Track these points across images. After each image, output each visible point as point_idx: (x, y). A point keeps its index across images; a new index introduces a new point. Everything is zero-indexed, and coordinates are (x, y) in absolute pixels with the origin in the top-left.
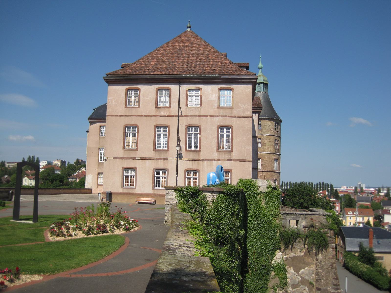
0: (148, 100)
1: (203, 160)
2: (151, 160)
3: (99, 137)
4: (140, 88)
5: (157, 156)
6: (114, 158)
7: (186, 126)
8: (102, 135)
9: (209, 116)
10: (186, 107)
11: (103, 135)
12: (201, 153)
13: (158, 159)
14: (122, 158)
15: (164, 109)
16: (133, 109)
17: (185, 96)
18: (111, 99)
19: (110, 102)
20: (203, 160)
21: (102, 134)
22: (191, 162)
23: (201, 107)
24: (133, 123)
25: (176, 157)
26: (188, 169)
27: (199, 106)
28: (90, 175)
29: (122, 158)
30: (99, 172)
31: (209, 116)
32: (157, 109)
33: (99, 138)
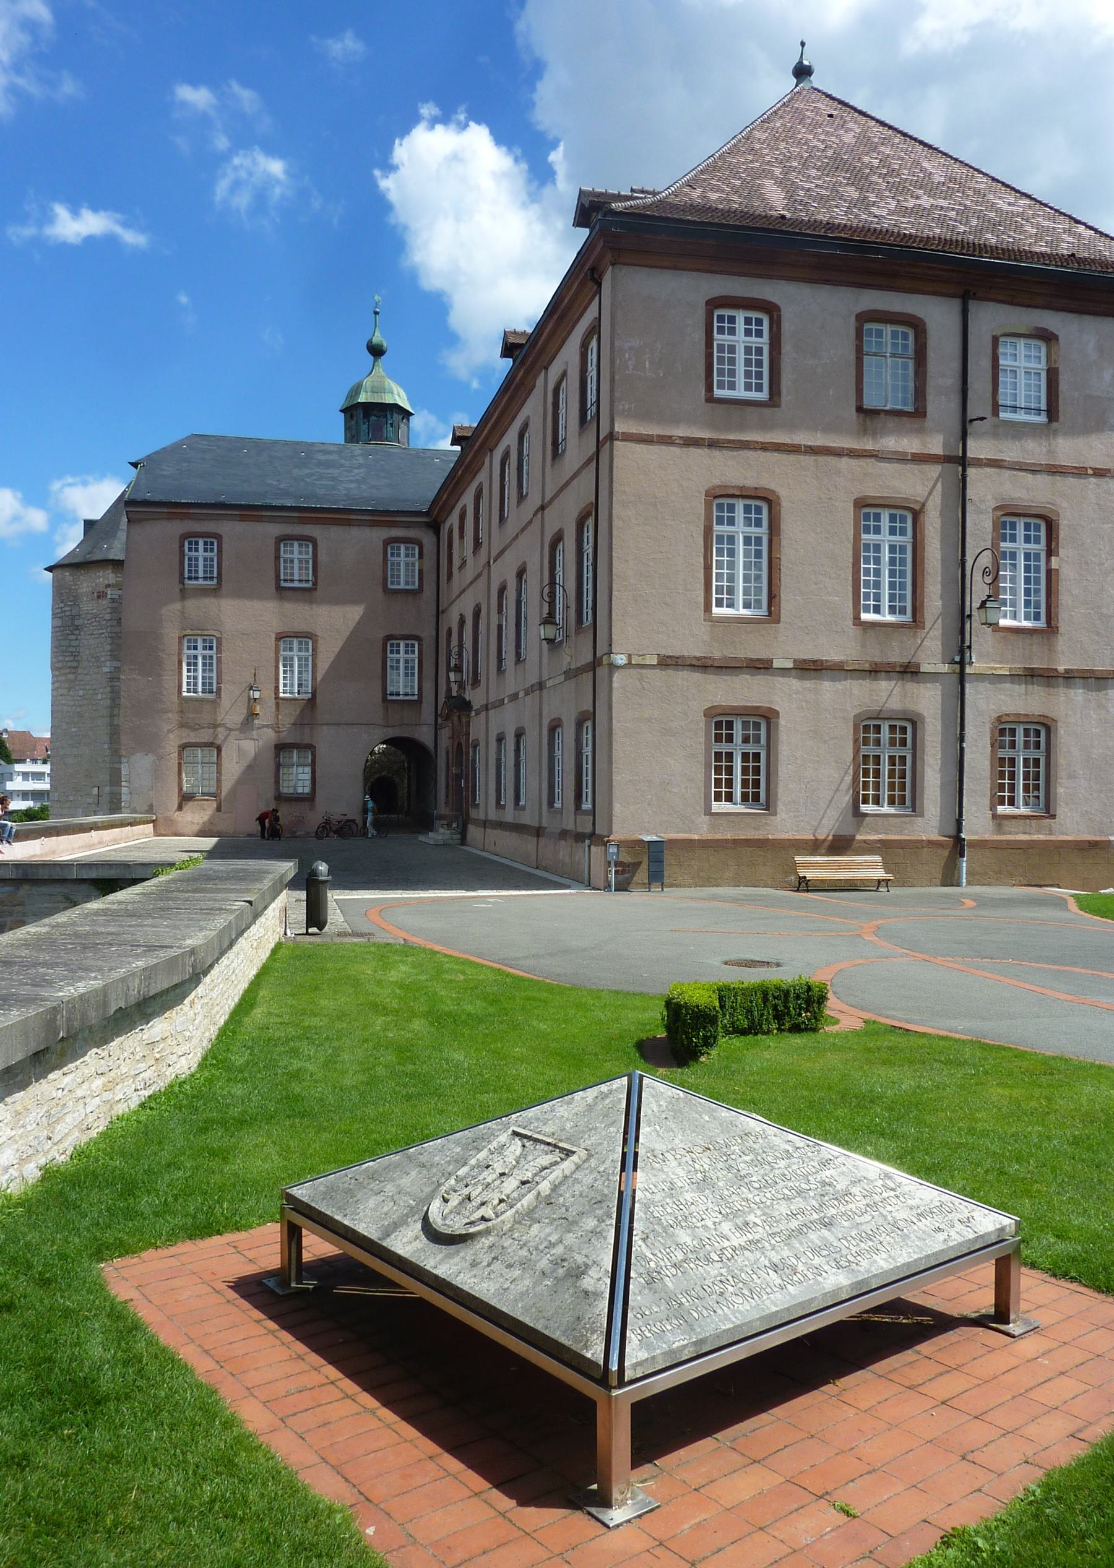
0: (819, 370)
1: (1069, 677)
2: (843, 672)
3: (181, 586)
4: (778, 303)
5: (875, 654)
6: (667, 662)
7: (995, 509)
8: (190, 578)
9: (1090, 472)
10: (995, 419)
11: (196, 578)
12: (1061, 643)
13: (875, 671)
14: (703, 666)
15: (896, 419)
16: (750, 409)
17: (986, 363)
18: (631, 348)
19: (630, 363)
20: (1069, 677)
21: (190, 571)
22: (1019, 689)
23: (1054, 425)
24: (750, 480)
25: (957, 659)
26: (1007, 715)
27: (1042, 418)
28: (138, 755)
29: (703, 666)
30: (184, 741)
31: (1090, 472)
32: (865, 421)
33: (181, 590)
